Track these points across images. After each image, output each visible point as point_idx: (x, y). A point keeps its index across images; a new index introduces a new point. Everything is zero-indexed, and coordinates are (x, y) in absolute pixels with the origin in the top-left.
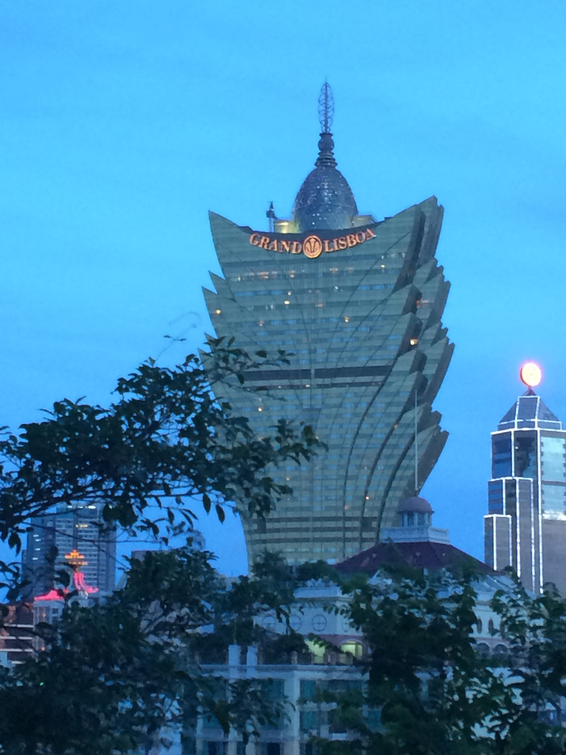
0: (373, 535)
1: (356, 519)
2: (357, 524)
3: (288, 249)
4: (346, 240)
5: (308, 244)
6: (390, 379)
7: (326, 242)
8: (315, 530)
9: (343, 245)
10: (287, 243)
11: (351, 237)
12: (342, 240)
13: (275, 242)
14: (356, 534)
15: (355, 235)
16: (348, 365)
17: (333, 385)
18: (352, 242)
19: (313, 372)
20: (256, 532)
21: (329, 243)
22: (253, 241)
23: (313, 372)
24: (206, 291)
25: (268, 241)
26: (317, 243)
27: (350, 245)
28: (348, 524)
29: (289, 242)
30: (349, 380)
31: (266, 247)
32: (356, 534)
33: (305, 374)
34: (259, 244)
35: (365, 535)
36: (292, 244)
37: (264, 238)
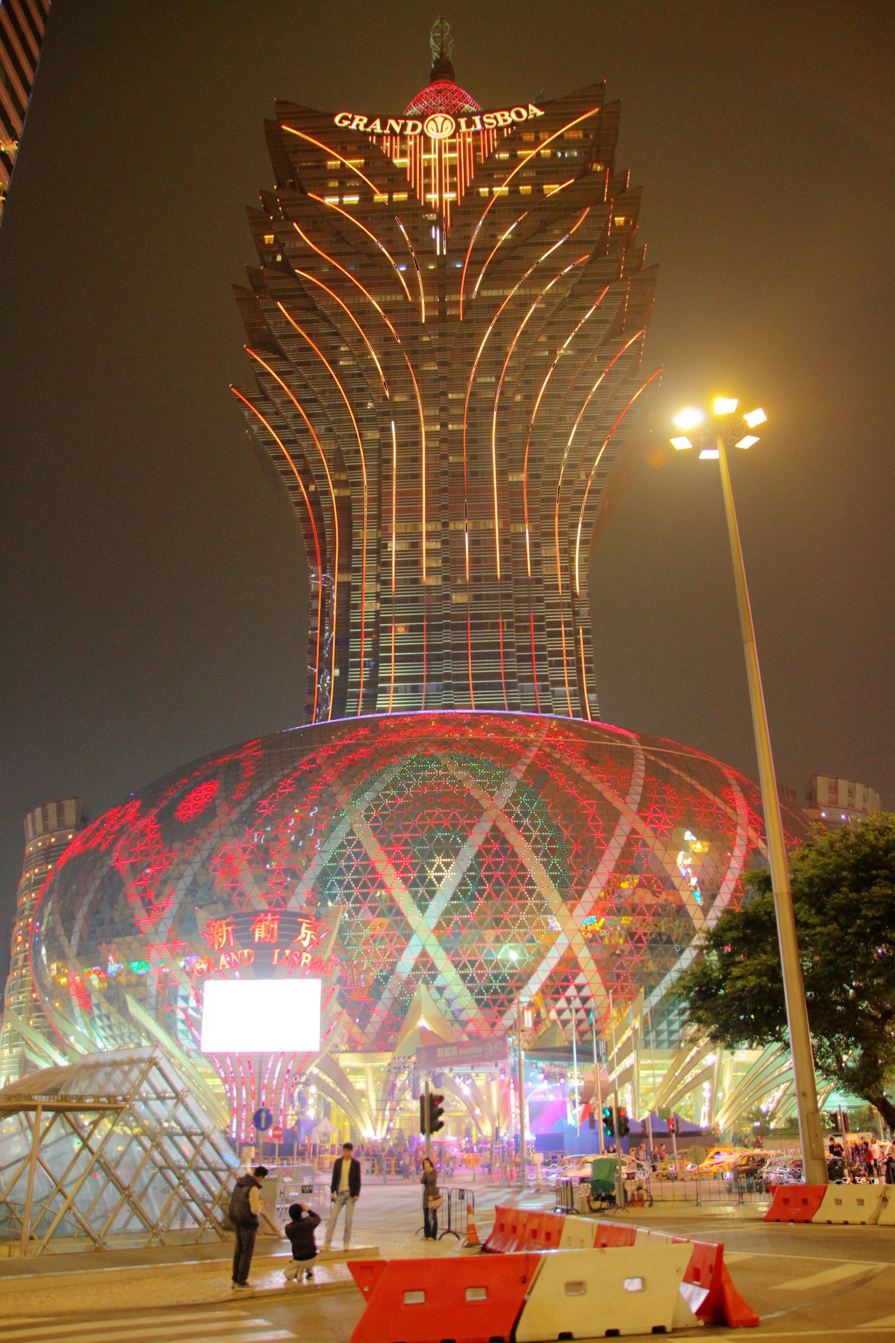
3: (397, 129)
4: (495, 118)
5: (432, 122)
7: (462, 121)
9: (491, 124)
10: (398, 124)
11: (503, 116)
12: (488, 118)
13: (378, 122)
15: (509, 112)
18: (505, 121)
21: (466, 122)
22: (340, 122)
25: (365, 120)
26: (447, 122)
27: (501, 123)
29: (401, 122)
31: (361, 128)
34: (351, 125)
36: (404, 127)
37: (357, 118)
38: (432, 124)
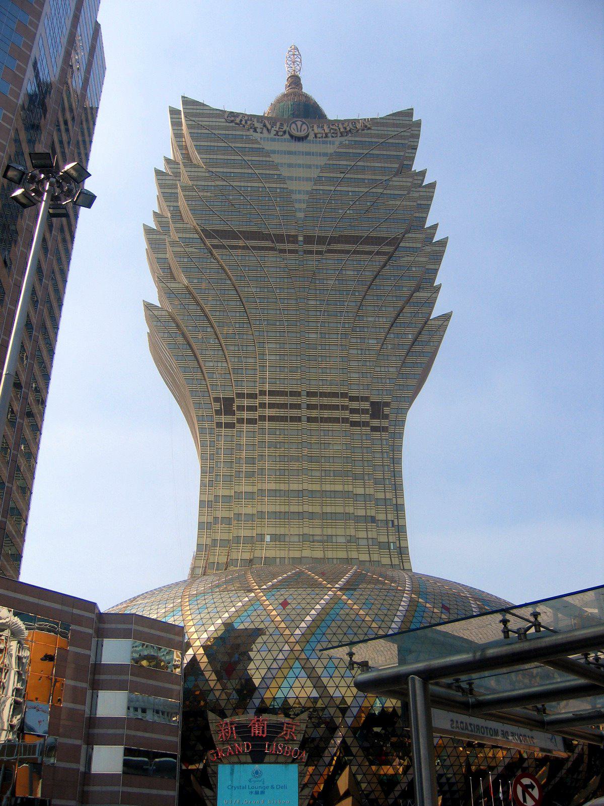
0: (385, 423)
1: (365, 399)
2: (366, 405)
6: (397, 254)
8: (310, 407)
14: (366, 418)
16: (346, 233)
17: (329, 251)
19: (301, 238)
20: (218, 412)
23: (301, 238)
24: (158, 173)
28: (355, 405)
30: (347, 247)
32: (366, 418)
33: (293, 239)
35: (375, 423)
38: (294, 126)
